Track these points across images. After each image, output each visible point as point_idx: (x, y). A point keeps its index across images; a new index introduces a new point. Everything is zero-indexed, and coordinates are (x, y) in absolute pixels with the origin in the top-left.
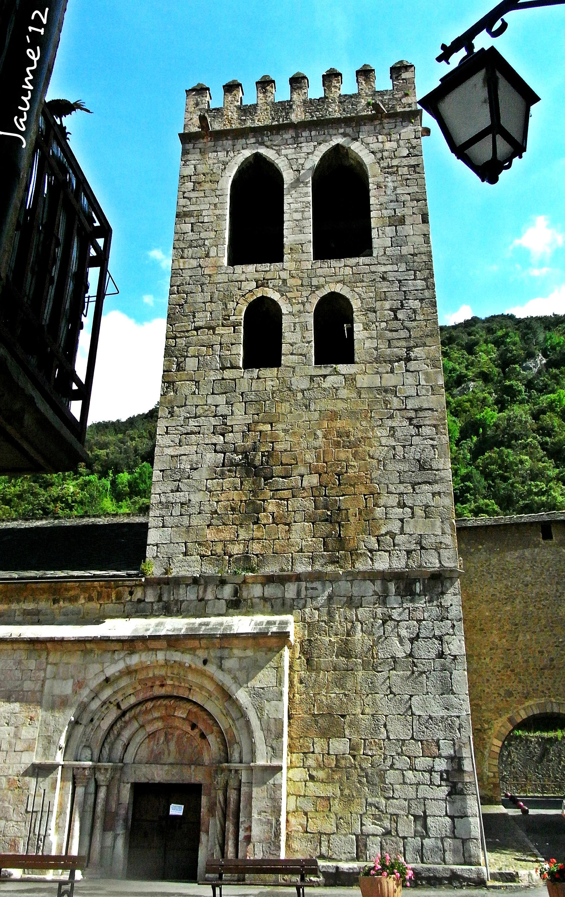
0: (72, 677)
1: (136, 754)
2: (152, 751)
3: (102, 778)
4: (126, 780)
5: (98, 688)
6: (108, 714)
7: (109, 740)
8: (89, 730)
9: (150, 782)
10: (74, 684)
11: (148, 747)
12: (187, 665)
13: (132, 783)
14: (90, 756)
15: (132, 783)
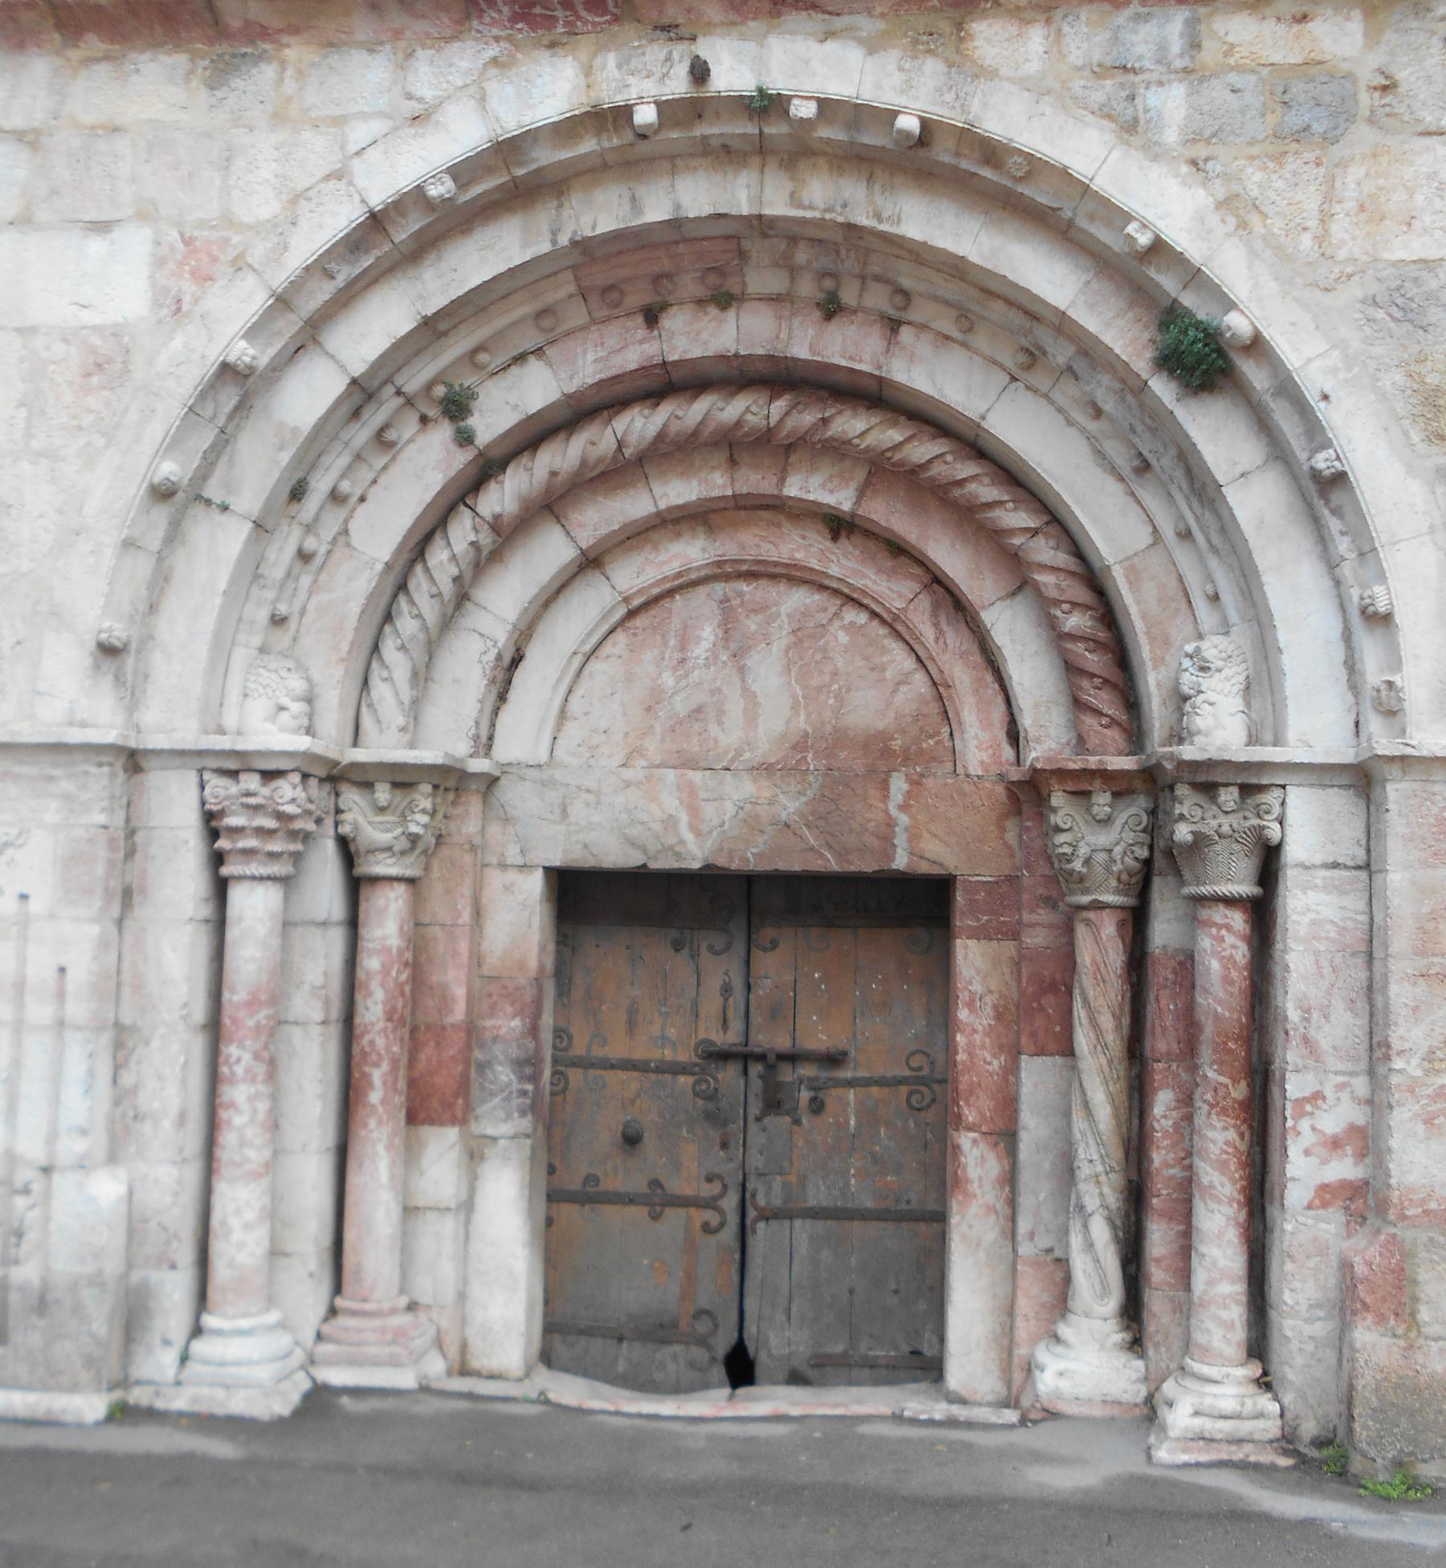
0: (145, 214)
1: (563, 715)
2: (653, 702)
3: (383, 837)
4: (513, 855)
5: (322, 292)
6: (395, 470)
7: (407, 625)
8: (280, 554)
9: (655, 865)
10: (160, 262)
11: (629, 678)
12: (908, 123)
13: (548, 870)
14: (297, 707)
15: (548, 870)
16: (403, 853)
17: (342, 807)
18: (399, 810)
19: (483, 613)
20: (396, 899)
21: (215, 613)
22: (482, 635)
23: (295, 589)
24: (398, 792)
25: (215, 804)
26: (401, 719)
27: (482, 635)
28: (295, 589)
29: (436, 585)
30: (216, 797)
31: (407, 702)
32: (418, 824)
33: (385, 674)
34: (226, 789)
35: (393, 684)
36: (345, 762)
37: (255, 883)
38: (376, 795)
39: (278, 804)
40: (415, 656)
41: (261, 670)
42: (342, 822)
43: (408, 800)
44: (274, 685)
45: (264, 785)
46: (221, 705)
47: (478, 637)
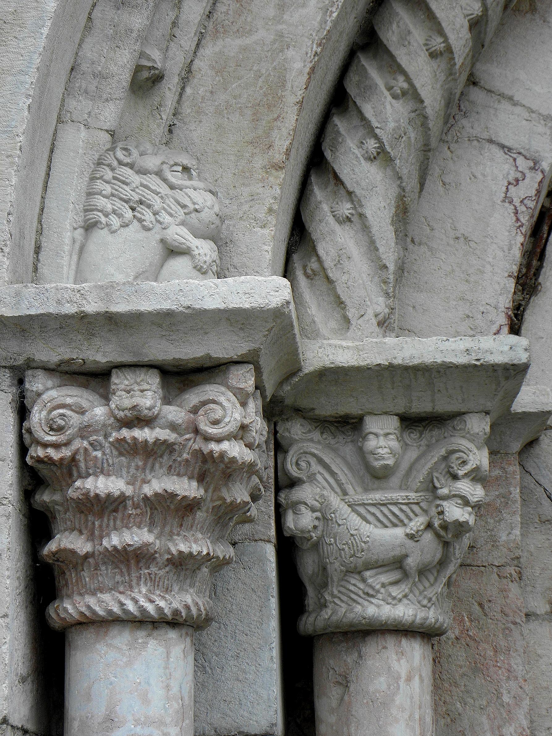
16: (422, 572)
17: (293, 471)
18: (421, 475)
19: (505, 105)
20: (409, 679)
21: (45, 31)
22: (506, 149)
23: (174, 24)
24: (411, 437)
25: (56, 446)
26: (381, 300)
27: (506, 149)
28: (174, 24)
29: (441, 32)
30: (60, 429)
31: (392, 267)
32: (466, 502)
33: (346, 209)
34: (82, 412)
35: (366, 228)
36: (306, 371)
37: (141, 634)
38: (372, 443)
39: (208, 439)
40: (404, 172)
41: (127, 171)
42: (295, 505)
43: (443, 452)
44: (157, 203)
45: (167, 401)
46: (38, 249)
47: (499, 154)
